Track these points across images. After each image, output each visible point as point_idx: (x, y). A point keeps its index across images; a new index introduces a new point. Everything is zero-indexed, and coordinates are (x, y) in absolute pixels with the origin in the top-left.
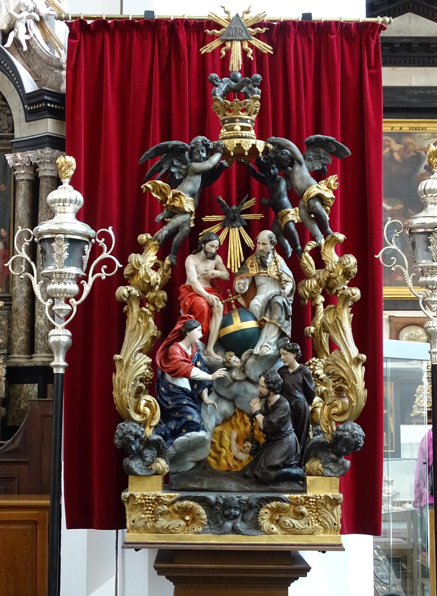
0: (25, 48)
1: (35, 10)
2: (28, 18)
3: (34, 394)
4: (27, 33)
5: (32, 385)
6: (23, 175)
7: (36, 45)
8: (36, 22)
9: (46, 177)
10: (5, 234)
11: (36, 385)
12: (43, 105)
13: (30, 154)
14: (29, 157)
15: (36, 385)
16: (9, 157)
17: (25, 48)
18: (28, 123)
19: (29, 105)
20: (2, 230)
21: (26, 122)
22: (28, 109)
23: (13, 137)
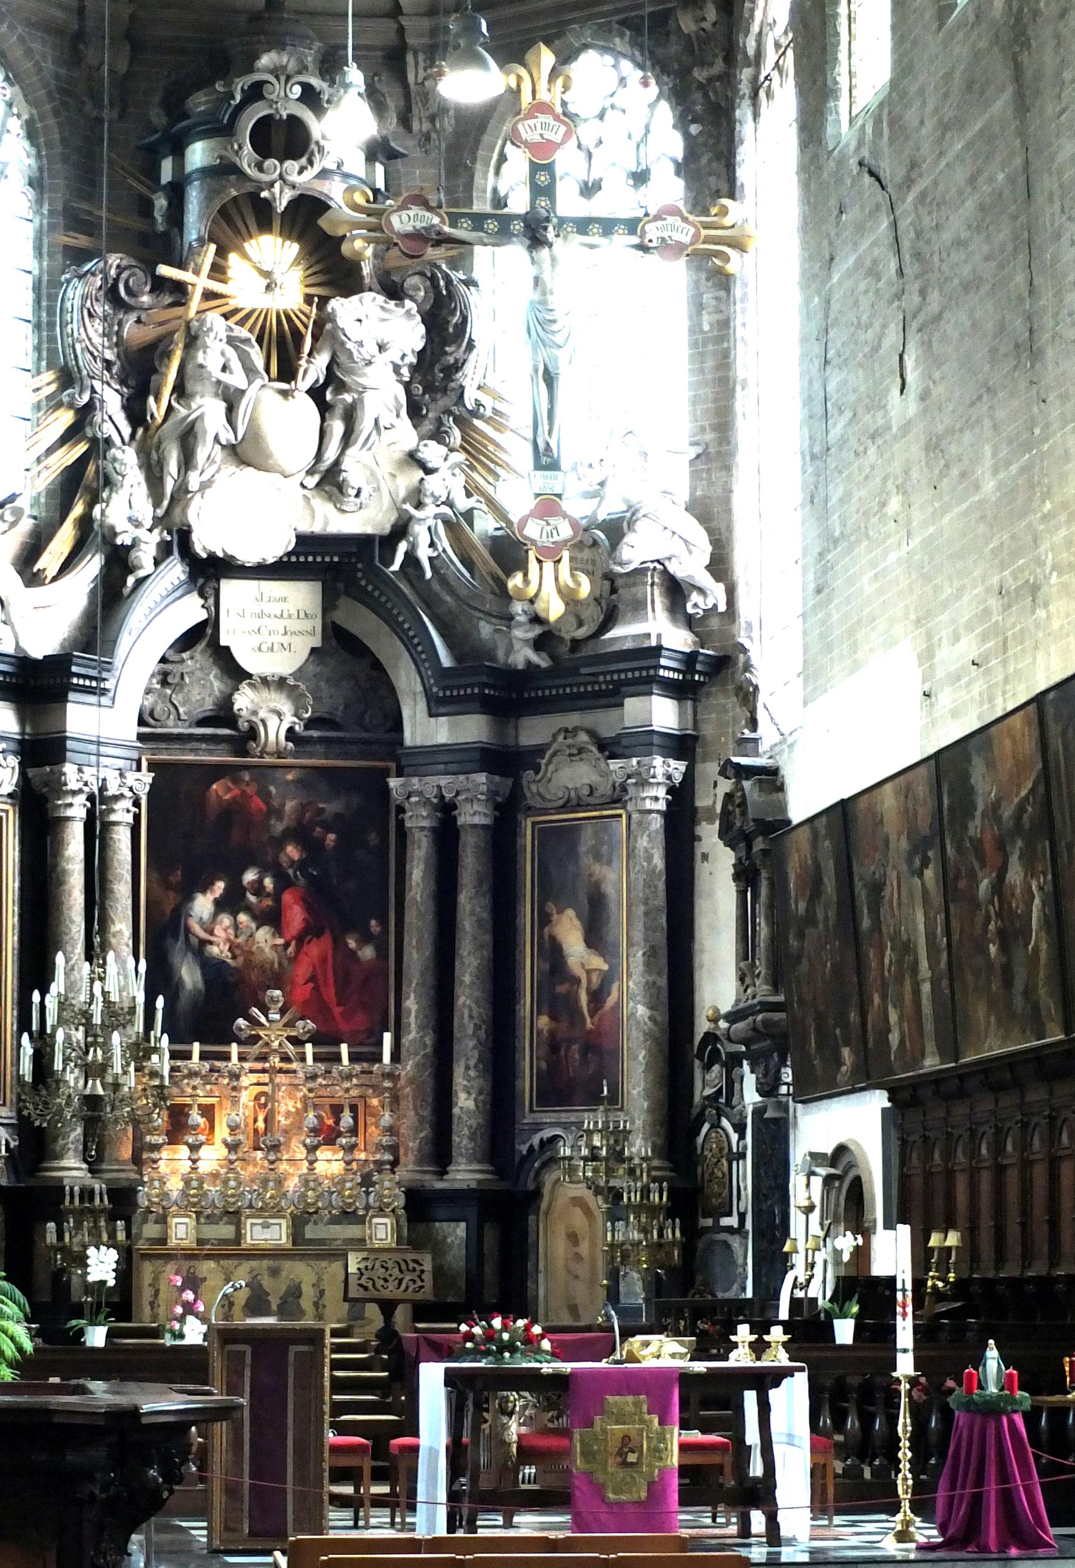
0: (429, 574)
1: (449, 503)
2: (436, 517)
3: (457, 1242)
4: (432, 545)
5: (453, 1224)
6: (419, 820)
7: (448, 568)
8: (447, 523)
9: (475, 826)
10: (378, 929)
11: (463, 1225)
12: (476, 691)
13: (444, 781)
14: (439, 787)
15: (463, 1225)
16: (394, 783)
17: (429, 574)
18: (433, 720)
19: (444, 689)
20: (373, 923)
21: (431, 715)
22: (441, 694)
23: (401, 742)
